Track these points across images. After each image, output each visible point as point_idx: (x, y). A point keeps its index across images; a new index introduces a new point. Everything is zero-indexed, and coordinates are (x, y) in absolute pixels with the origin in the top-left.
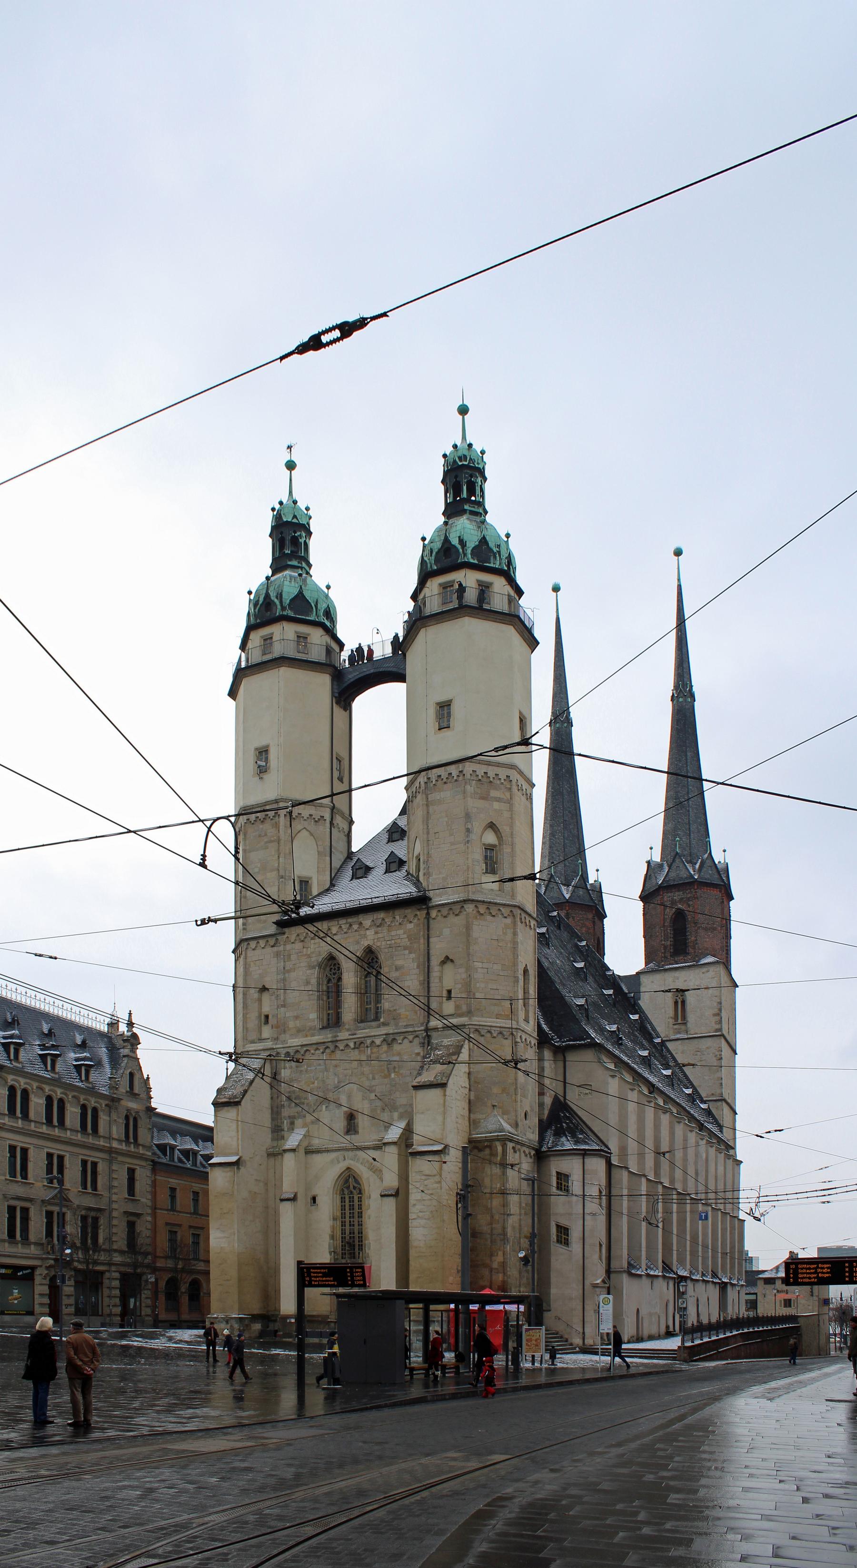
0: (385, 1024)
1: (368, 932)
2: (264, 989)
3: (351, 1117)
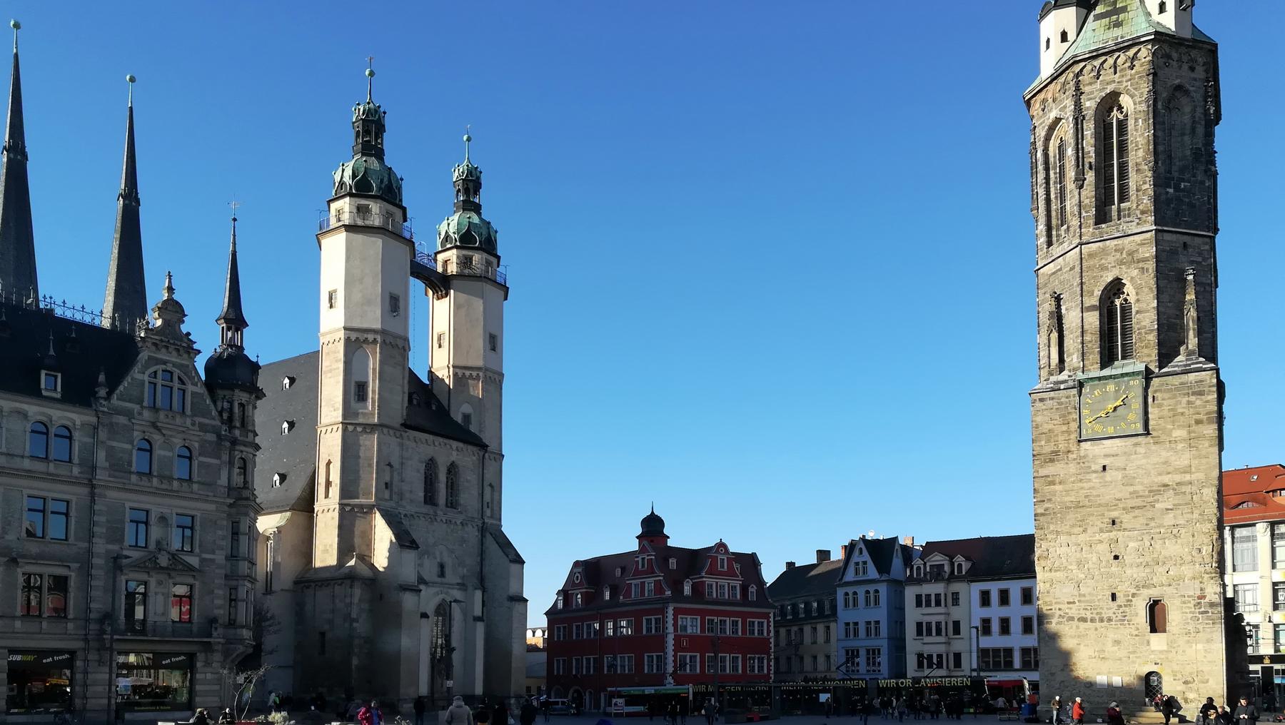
0: (461, 513)
1: (453, 452)
2: (389, 465)
3: (442, 566)
